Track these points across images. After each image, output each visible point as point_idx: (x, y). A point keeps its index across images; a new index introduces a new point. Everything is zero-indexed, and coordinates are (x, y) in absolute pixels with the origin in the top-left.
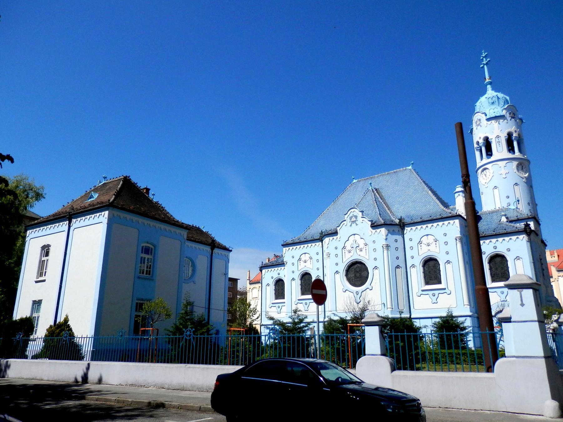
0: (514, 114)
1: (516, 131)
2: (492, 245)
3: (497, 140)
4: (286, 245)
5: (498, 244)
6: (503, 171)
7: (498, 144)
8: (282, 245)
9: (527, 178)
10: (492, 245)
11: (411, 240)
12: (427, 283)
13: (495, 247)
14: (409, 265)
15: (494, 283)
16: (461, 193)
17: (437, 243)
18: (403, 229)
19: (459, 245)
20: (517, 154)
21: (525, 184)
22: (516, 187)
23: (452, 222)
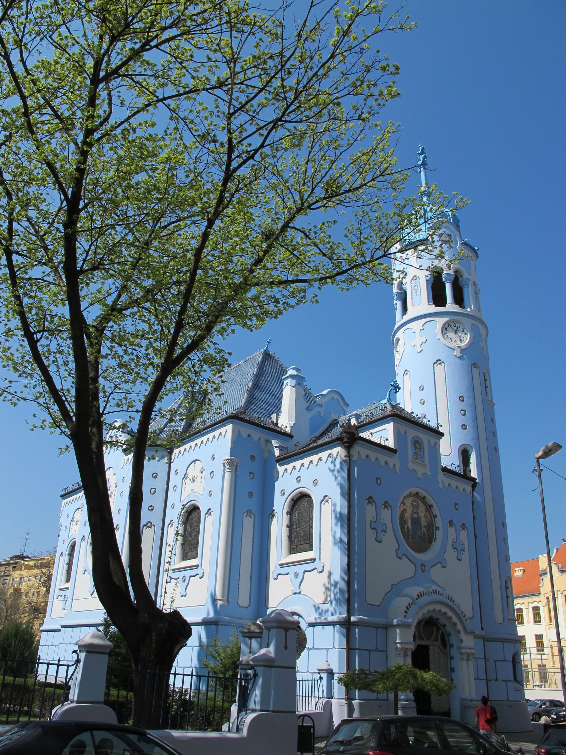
0: (450, 236)
1: (449, 267)
2: (296, 474)
3: (413, 284)
4: (64, 496)
5: (304, 473)
6: (418, 340)
7: (414, 291)
8: (62, 496)
9: (462, 350)
10: (296, 474)
11: (176, 472)
12: (185, 557)
13: (298, 479)
14: (167, 522)
15: (292, 555)
16: (289, 381)
17: (203, 475)
18: (171, 453)
19: (228, 475)
20: (450, 306)
21: (458, 361)
22: (438, 368)
23: (223, 430)
